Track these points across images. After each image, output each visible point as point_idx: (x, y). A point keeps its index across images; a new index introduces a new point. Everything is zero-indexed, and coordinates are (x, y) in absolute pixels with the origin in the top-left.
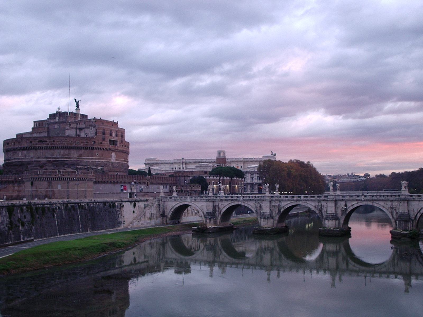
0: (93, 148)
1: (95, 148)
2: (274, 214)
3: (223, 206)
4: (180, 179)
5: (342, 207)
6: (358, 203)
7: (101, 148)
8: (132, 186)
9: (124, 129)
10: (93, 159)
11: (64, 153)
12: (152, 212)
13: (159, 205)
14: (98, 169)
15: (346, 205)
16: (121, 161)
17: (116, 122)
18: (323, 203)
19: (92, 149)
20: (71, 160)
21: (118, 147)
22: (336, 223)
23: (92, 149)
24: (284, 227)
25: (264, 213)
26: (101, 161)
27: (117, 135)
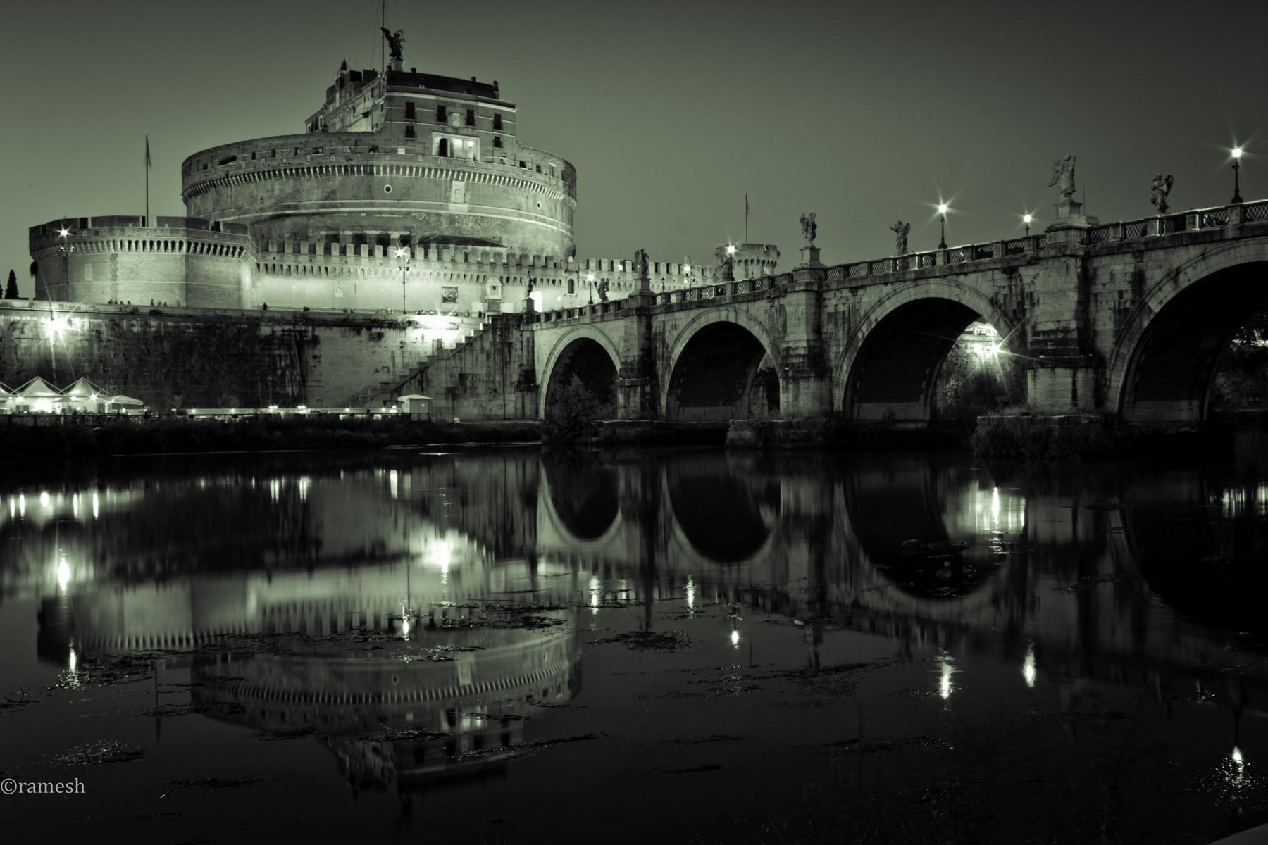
0: (372, 166)
1: (378, 167)
2: (832, 357)
3: (675, 333)
5: (1121, 293)
6: (1204, 256)
8: (488, 289)
10: (372, 205)
12: (468, 371)
13: (510, 345)
15: (1138, 279)
18: (1027, 274)
20: (303, 211)
22: (1074, 384)
24: (920, 425)
25: (788, 349)
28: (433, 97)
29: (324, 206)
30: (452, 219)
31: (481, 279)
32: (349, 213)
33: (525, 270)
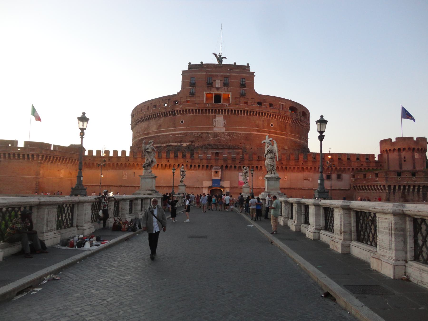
0: (174, 111)
1: (177, 111)
4: (388, 156)
7: (186, 110)
8: (213, 173)
9: (254, 73)
10: (175, 130)
11: (144, 127)
14: (183, 146)
16: (245, 130)
17: (246, 65)
19: (174, 113)
20: (151, 136)
21: (229, 105)
23: (174, 113)
26: (189, 132)
27: (226, 85)
28: (205, 73)
29: (156, 132)
30: (216, 135)
31: (209, 168)
32: (166, 135)
33: (238, 162)
